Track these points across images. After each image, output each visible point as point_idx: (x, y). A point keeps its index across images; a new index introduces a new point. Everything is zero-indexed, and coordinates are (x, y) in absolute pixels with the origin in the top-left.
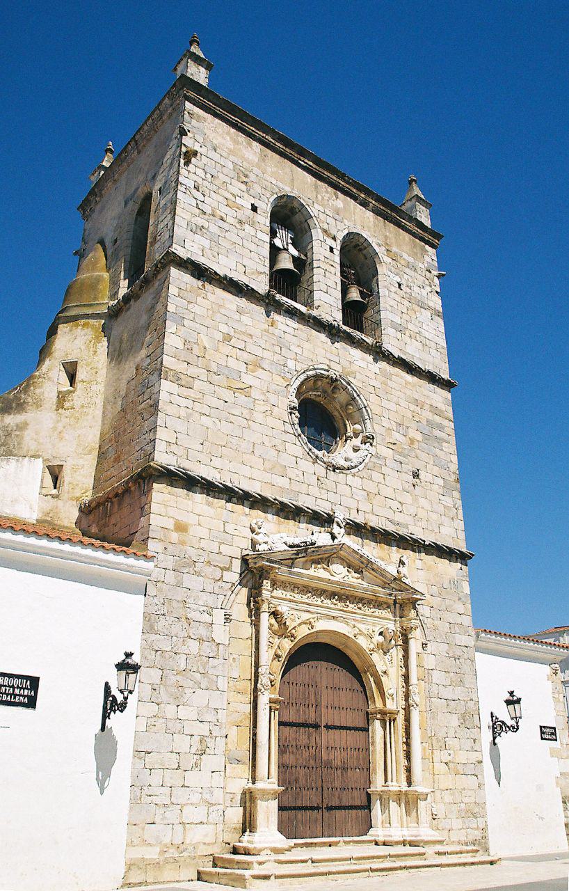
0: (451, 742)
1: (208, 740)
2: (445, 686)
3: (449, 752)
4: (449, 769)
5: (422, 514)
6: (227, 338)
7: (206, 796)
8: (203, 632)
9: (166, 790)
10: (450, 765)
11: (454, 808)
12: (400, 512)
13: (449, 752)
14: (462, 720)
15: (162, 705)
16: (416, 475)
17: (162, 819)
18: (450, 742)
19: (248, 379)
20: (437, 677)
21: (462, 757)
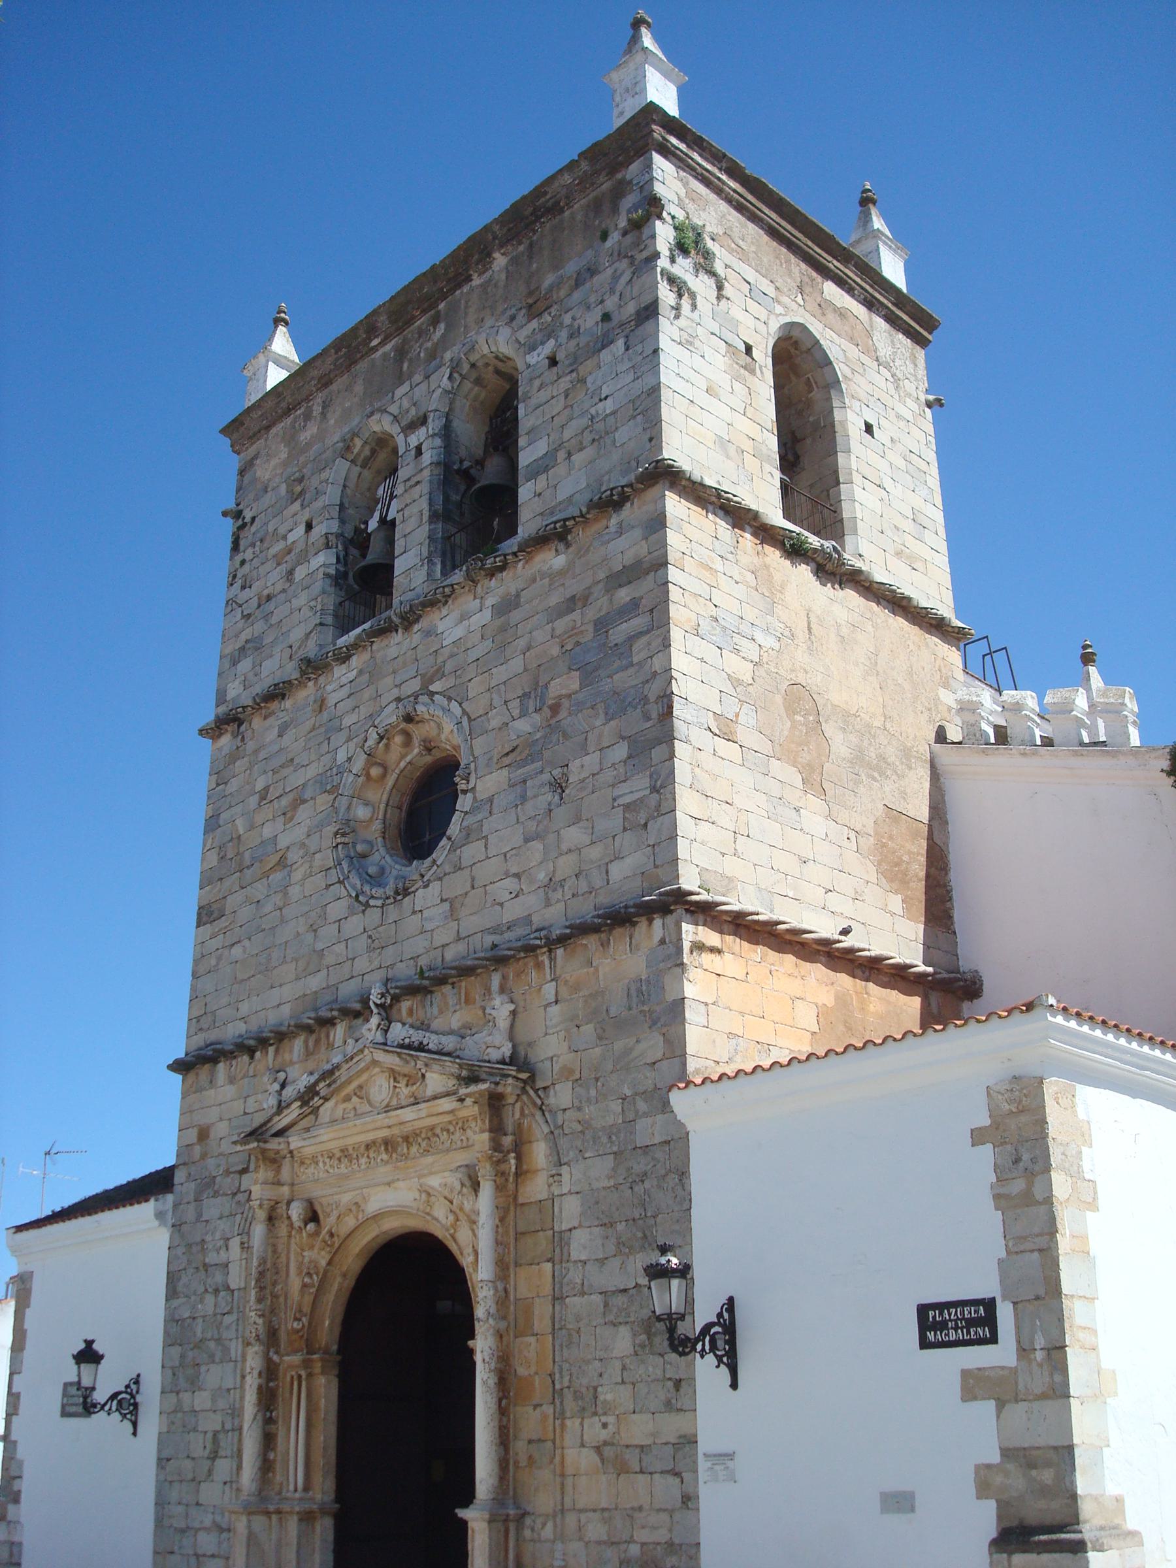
0: (609, 1397)
1: (221, 1436)
2: (602, 1262)
3: (604, 1419)
4: (602, 1460)
5: (566, 866)
6: (264, 795)
7: (218, 1518)
8: (219, 1278)
9: (181, 1509)
10: (608, 1452)
11: (609, 1553)
12: (517, 896)
13: (604, 1419)
14: (644, 1337)
15: (181, 1395)
16: (559, 786)
17: (180, 1548)
18: (606, 1395)
19: (283, 842)
20: (582, 1244)
21: (639, 1429)
